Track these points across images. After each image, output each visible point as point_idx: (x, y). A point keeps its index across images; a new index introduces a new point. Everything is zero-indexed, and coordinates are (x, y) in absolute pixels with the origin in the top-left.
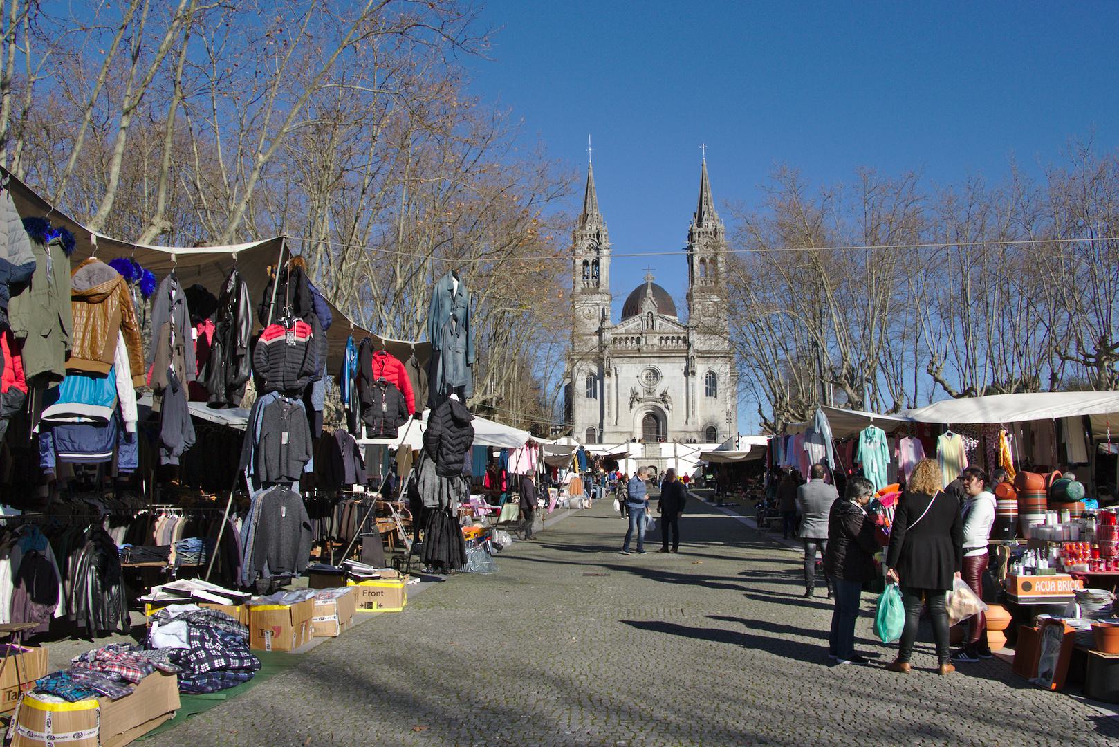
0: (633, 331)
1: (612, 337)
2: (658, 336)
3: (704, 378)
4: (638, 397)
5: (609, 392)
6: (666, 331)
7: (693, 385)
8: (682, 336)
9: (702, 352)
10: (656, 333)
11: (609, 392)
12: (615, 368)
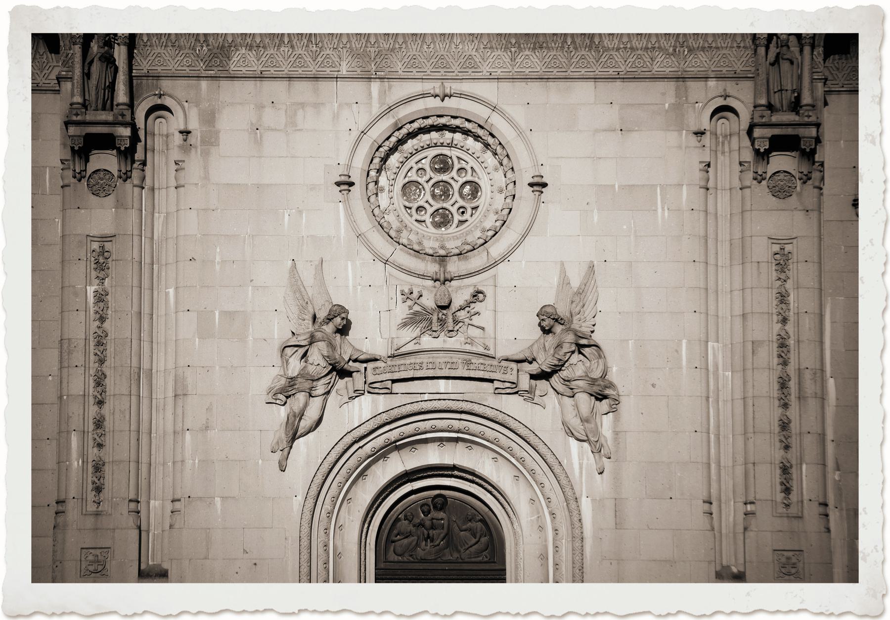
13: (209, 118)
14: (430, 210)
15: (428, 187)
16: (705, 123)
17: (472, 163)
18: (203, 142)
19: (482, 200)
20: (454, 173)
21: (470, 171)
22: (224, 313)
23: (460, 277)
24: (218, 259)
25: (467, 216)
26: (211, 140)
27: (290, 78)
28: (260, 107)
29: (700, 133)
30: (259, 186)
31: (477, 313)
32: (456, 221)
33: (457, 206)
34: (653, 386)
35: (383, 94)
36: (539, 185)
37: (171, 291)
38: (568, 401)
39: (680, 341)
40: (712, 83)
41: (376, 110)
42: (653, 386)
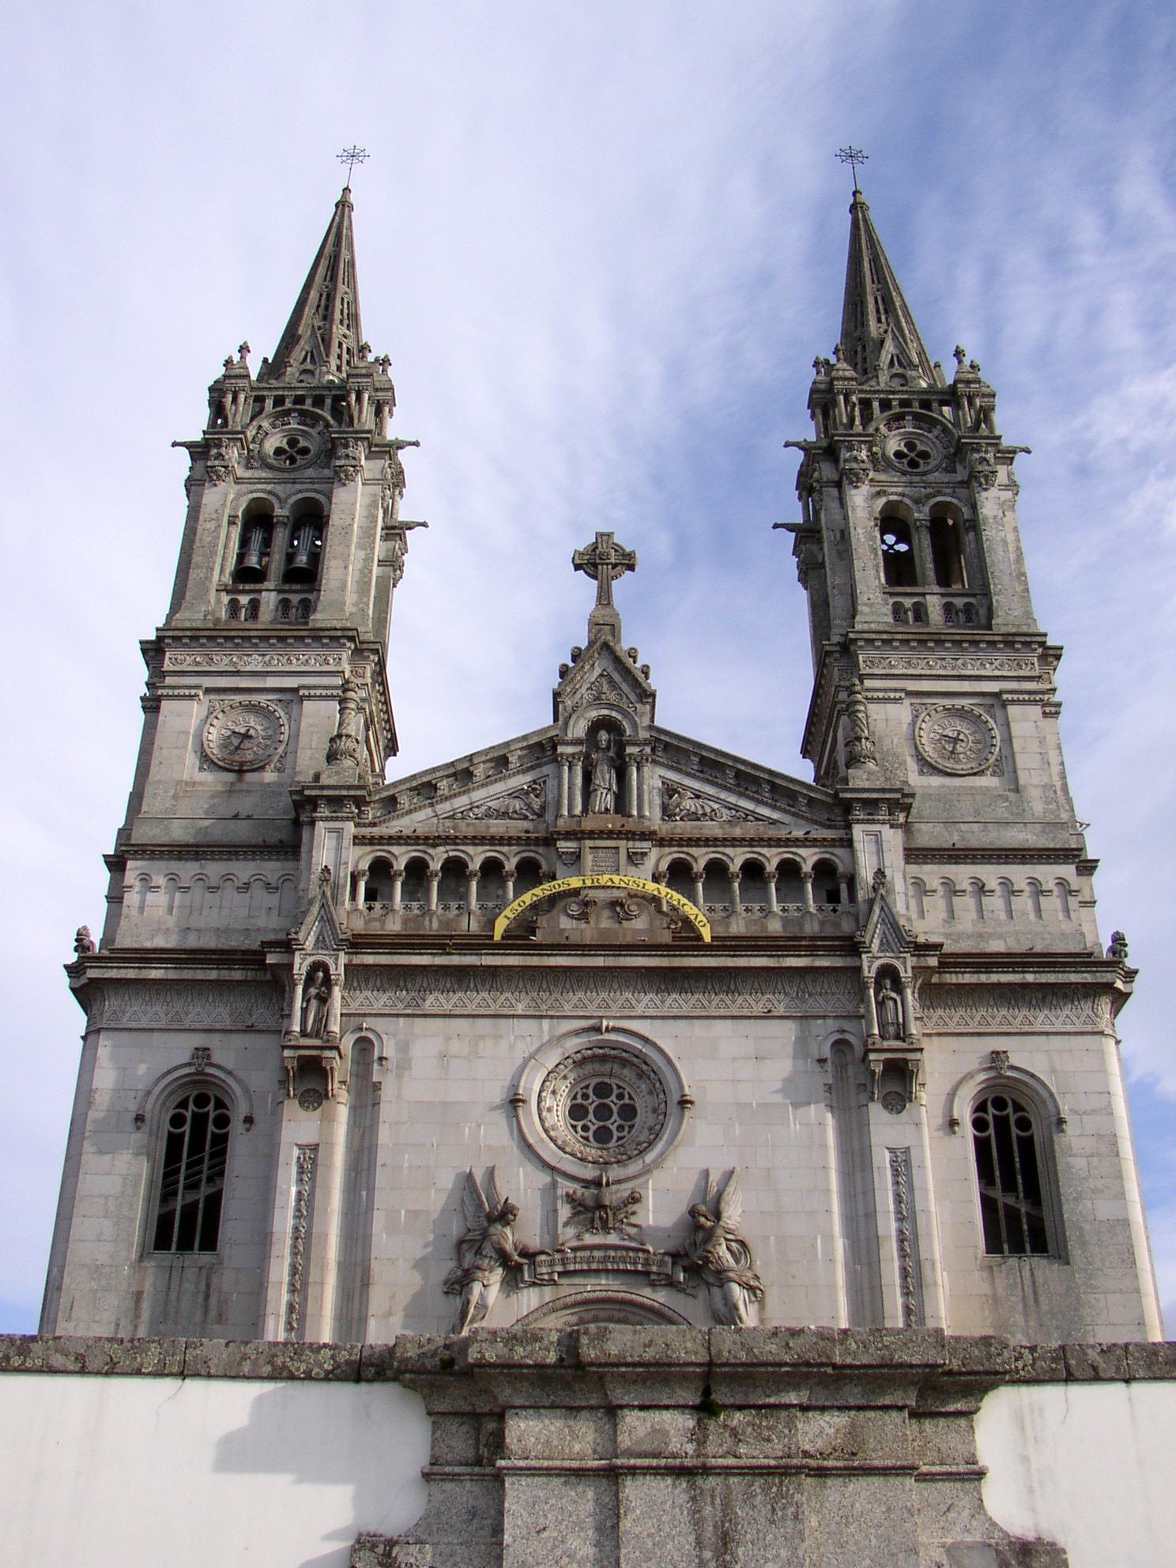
0: (497, 827)
1: (360, 858)
2: (658, 858)
3: (968, 1131)
4: (509, 1238)
5: (306, 1206)
6: (712, 829)
7: (902, 1163)
8: (808, 858)
9: (952, 962)
10: (647, 836)
11: (306, 1206)
12: (364, 1045)
13: (404, 1048)
14: (593, 1128)
15: (591, 1109)
16: (827, 1052)
17: (628, 1089)
18: (398, 1067)
19: (637, 1119)
20: (613, 1097)
21: (627, 1096)
22: (407, 1211)
23: (619, 1182)
24: (406, 1165)
25: (625, 1133)
26: (405, 1065)
27: (474, 1016)
28: (448, 1038)
29: (822, 1061)
30: (445, 1104)
31: (634, 1213)
32: (615, 1138)
33: (616, 1124)
34: (793, 1277)
35: (552, 1028)
36: (684, 1103)
37: (364, 1193)
38: (716, 1291)
39: (816, 1238)
40: (830, 1022)
41: (546, 1038)
42: (793, 1277)
